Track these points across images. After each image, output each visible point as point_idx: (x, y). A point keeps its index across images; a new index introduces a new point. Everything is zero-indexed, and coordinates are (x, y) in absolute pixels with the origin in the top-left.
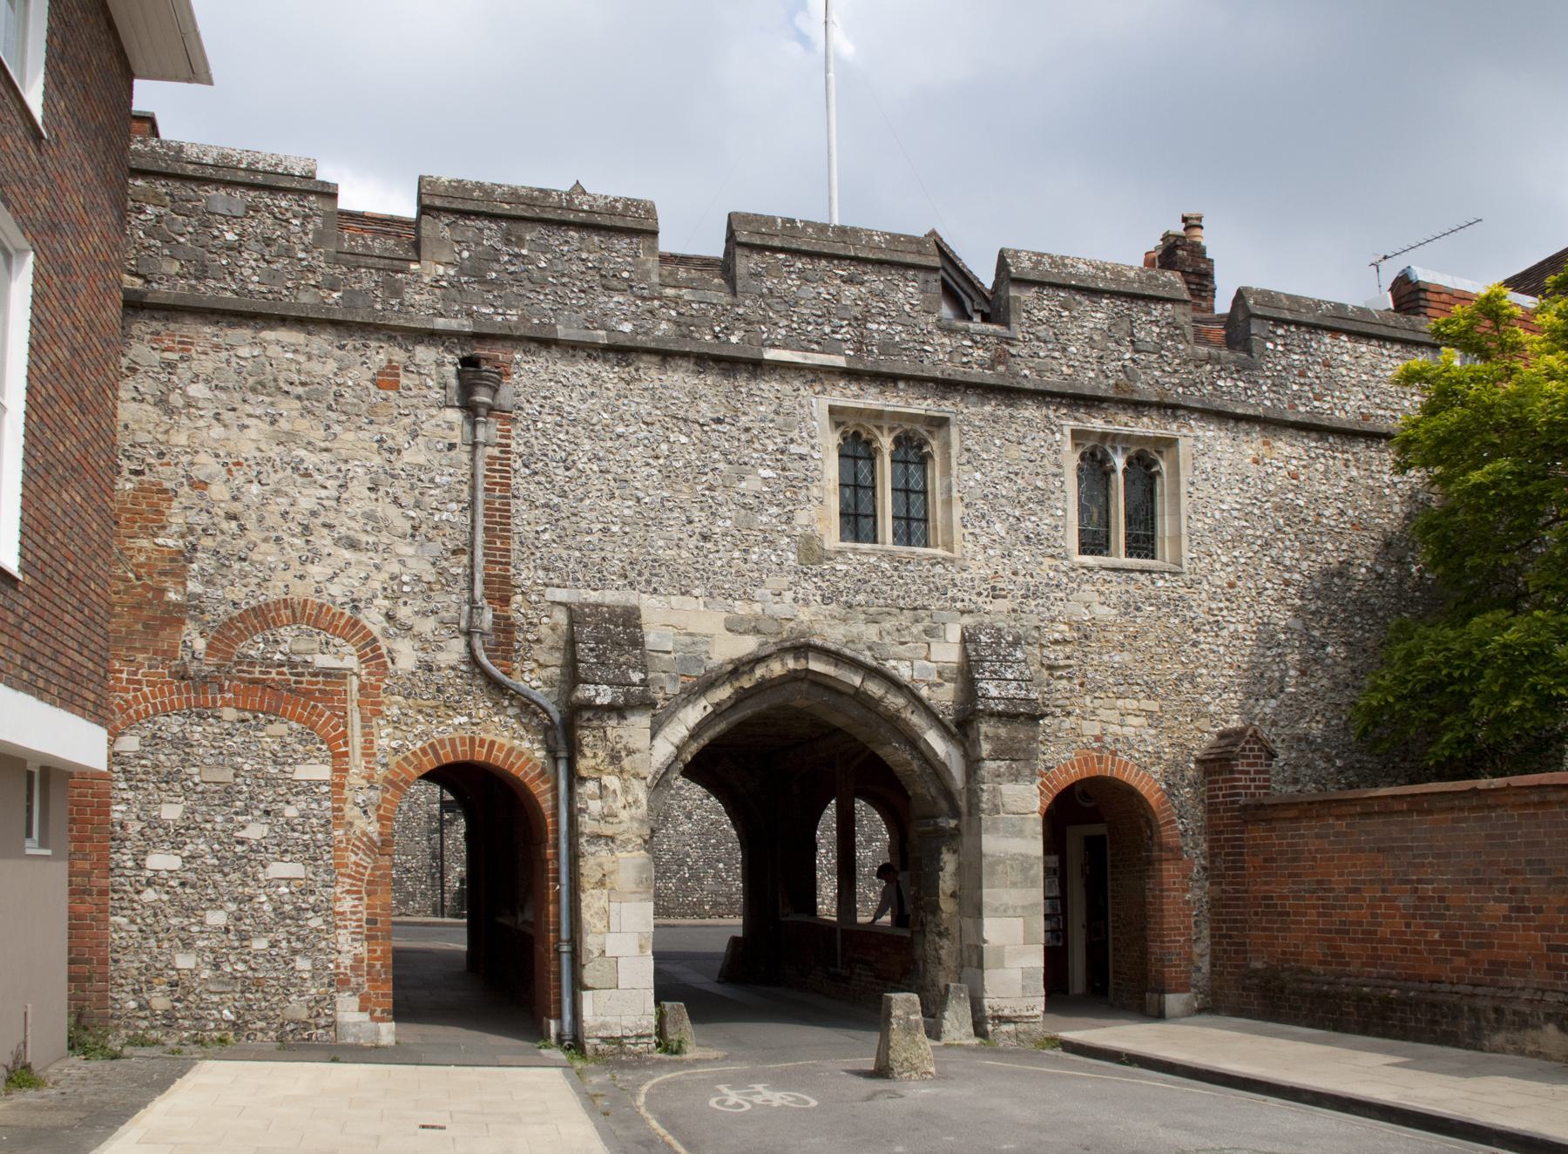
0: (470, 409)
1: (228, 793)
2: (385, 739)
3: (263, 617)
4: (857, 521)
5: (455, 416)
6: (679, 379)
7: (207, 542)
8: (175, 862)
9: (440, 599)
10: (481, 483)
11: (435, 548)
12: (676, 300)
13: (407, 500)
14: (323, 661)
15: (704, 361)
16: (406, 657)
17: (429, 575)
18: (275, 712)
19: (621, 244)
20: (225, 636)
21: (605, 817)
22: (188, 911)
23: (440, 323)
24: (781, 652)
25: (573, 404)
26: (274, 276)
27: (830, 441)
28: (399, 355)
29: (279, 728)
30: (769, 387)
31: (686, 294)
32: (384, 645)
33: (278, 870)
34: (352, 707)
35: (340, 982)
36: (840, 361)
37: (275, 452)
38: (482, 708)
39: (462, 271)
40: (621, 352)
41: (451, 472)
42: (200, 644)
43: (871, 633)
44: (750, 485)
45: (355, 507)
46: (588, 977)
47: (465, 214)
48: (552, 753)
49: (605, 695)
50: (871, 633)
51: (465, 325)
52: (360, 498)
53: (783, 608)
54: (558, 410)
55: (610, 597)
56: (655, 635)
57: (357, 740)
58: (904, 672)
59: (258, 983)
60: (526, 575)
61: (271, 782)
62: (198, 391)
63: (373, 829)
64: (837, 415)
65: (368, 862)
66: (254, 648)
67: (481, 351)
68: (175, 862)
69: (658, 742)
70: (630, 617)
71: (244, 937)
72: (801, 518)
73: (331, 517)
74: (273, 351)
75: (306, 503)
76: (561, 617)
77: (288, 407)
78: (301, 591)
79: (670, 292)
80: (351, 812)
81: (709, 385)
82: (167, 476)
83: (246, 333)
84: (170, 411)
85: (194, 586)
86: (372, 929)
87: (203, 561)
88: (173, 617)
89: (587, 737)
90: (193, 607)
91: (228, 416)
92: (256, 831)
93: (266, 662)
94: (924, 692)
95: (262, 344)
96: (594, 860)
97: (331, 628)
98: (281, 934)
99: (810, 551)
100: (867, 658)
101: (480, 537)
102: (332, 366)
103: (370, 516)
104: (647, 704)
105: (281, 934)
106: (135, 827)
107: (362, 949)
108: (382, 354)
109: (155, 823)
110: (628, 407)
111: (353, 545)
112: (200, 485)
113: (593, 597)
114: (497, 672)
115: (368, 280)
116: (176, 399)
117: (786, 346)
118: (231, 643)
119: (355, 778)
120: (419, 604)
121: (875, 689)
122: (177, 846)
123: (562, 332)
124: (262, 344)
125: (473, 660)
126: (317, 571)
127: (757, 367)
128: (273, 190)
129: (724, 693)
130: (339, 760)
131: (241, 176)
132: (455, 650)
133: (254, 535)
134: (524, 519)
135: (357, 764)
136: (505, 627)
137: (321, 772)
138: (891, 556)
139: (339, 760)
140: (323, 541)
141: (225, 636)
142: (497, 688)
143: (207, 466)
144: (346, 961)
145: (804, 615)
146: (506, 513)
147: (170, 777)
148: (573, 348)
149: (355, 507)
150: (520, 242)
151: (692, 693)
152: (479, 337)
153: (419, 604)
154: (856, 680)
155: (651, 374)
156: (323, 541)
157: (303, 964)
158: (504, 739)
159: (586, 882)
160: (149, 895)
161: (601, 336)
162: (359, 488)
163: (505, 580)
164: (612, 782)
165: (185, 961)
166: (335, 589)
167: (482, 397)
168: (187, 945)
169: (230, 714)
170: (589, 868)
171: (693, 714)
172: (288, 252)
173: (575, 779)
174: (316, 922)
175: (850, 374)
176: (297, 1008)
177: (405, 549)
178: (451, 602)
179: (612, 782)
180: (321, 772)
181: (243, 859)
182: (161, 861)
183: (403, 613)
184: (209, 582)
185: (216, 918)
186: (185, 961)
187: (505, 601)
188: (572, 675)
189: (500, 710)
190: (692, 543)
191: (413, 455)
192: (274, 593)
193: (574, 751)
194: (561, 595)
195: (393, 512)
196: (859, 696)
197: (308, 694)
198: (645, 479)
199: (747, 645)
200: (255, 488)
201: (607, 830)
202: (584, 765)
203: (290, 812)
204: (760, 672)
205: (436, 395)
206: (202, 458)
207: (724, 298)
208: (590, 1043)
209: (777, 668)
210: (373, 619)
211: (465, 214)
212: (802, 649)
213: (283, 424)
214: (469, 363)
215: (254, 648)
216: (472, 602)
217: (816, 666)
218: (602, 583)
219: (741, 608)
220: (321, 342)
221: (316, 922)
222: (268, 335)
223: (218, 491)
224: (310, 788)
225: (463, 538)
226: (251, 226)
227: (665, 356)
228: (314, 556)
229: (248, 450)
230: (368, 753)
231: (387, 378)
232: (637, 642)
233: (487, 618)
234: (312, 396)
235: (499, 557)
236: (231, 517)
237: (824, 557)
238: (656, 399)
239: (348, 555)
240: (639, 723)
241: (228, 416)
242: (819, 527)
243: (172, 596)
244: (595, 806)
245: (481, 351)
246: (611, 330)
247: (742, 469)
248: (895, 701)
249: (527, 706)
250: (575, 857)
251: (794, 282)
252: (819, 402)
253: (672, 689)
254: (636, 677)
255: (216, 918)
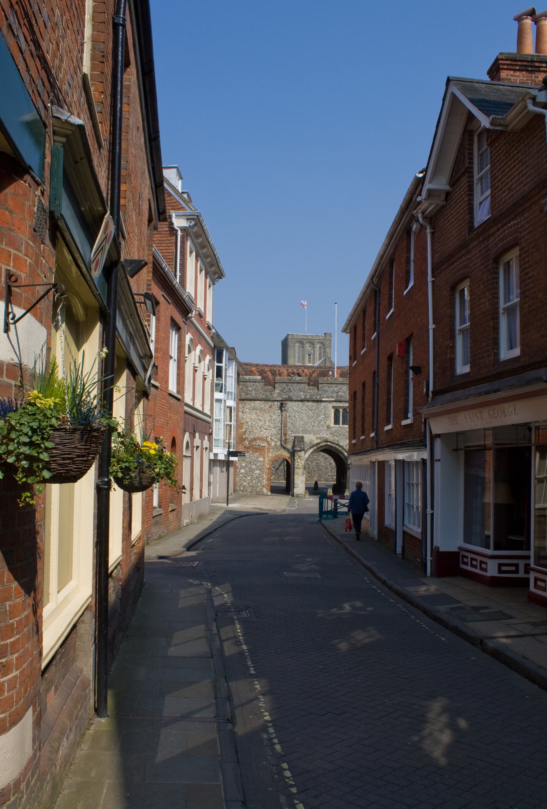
0: (282, 411)
1: (250, 462)
2: (270, 455)
3: (255, 439)
4: (336, 422)
5: (279, 411)
6: (310, 404)
7: (248, 430)
8: (244, 471)
9: (277, 436)
10: (283, 420)
11: (277, 429)
12: (310, 393)
13: (273, 423)
14: (263, 445)
15: (314, 401)
16: (273, 444)
17: (276, 433)
18: (256, 452)
19: (303, 385)
20: (250, 442)
21: (298, 465)
22: (245, 477)
23: (278, 399)
24: (324, 442)
25: (295, 408)
26: (256, 394)
27: (333, 411)
28: (272, 404)
29: (257, 454)
30: (323, 404)
31: (311, 391)
32: (270, 442)
33: (257, 472)
34: (266, 451)
35: (264, 486)
36: (333, 399)
37: (256, 417)
38: (283, 450)
39: (280, 391)
40: (302, 401)
41: (279, 419)
42: (247, 443)
43: (337, 439)
44: (320, 418)
45: (267, 424)
46: (295, 486)
47: (281, 383)
48: (292, 456)
49: (298, 449)
50: (337, 439)
51: (281, 399)
52: (267, 423)
53: (324, 435)
54: (293, 409)
55: (300, 435)
56: (306, 440)
57: (267, 455)
58: (342, 444)
59: (254, 487)
60: (289, 432)
61: (256, 461)
62: (246, 410)
63: (268, 466)
64: (333, 407)
65: (267, 471)
66: (254, 443)
67: (283, 402)
68: (244, 471)
69: (306, 455)
70: (302, 438)
71: (252, 480)
72: (327, 422)
73: (264, 426)
74: (256, 404)
75: (260, 424)
76: (293, 438)
77: (258, 412)
78: (260, 436)
79: (309, 391)
80: (266, 464)
81: (314, 404)
82: (243, 421)
83: (253, 402)
84: (243, 413)
85: (247, 436)
86: (269, 479)
87: (248, 432)
88: (244, 440)
89: (296, 454)
90: (246, 438)
91: (251, 413)
92: (254, 467)
93: (255, 445)
94: (345, 447)
95: (255, 403)
96: (296, 471)
97: (264, 440)
98: (257, 480)
99: (328, 427)
100: (336, 442)
101: (283, 428)
102: (264, 406)
103: (269, 425)
104: (304, 450)
105: (257, 480)
106: (239, 467)
107: (266, 482)
108: (270, 403)
109: (242, 466)
110: (303, 408)
111: (266, 429)
112: (247, 423)
113: (298, 435)
114: (284, 446)
115: (268, 393)
116: (244, 411)
117: (326, 398)
118: (251, 443)
119: (266, 460)
120: (275, 437)
121: (337, 447)
122: (244, 469)
123: (294, 399)
124: (255, 403)
125: (281, 444)
126: (262, 433)
127: (321, 401)
128: (256, 382)
129: (315, 448)
130: (264, 458)
131: (252, 381)
132: (279, 443)
133: (254, 429)
134: (289, 425)
135: (267, 458)
136: (286, 439)
137: (262, 459)
138: (340, 427)
139: (264, 458)
140: (263, 429)
141: (250, 442)
142: (285, 448)
143: (248, 420)
144: (265, 484)
145: (327, 436)
146: (286, 424)
147: (244, 460)
148: (295, 401)
149: (267, 424)
150: (288, 386)
151: (310, 448)
152: (283, 400)
153: (275, 437)
154: (335, 445)
155: (307, 404)
156: (263, 429)
157: (259, 484)
158: (285, 454)
159: (295, 474)
160: (241, 475)
161: (299, 399)
162: (267, 422)
163: (286, 433)
164: (299, 460)
165: (245, 484)
166: (264, 435)
167: (283, 409)
168: (245, 481)
169: (251, 452)
170: (296, 472)
171: (311, 451)
172: (258, 391)
173: (294, 460)
174: (261, 479)
175: (335, 401)
176: (258, 490)
177: (273, 430)
178: (279, 436)
179: (299, 460)
180: (262, 459)
181: (252, 471)
182: (242, 471)
183: (273, 438)
184: (248, 435)
185: (249, 478)
186: (245, 484)
187: (286, 436)
188: (294, 446)
189: (285, 451)
190: (312, 427)
191: (274, 417)
192: (257, 436)
193: (294, 456)
194: (293, 435)
195: (271, 425)
196: (335, 448)
197: (261, 449)
198: (305, 418)
199: (319, 441)
200: (254, 423)
201: (298, 467)
202: (295, 458)
203: (258, 464)
204: (320, 444)
205: (277, 409)
206: (248, 419)
207: (317, 391)
208: (295, 495)
209: (323, 444)
210: (269, 439)
211: (281, 383)
212: (327, 441)
213: (258, 414)
214: (282, 404)
215: (254, 443)
216: (281, 436)
217: (329, 444)
218: (299, 433)
219: (318, 436)
220: (262, 402)
221: (261, 479)
222: (256, 402)
223: (250, 423)
224: (260, 461)
225: (280, 428)
226: (253, 387)
227: (308, 401)
228: (261, 431)
229: (253, 418)
230: (268, 457)
231: (271, 407)
232: (303, 441)
233: (283, 439)
234: (261, 410)
235: (285, 430)
236: (251, 426)
237: (331, 428)
238: (307, 407)
239: (266, 431)
240: (303, 452)
241: (251, 413)
242: (330, 424)
243: (244, 437)
244: (296, 464)
245: (283, 402)
246: (301, 398)
247: (319, 416)
248: (340, 448)
249: (288, 450)
250: (294, 470)
251: (327, 388)
252: (330, 405)
253: (308, 447)
254: (302, 446)
255: (249, 478)
